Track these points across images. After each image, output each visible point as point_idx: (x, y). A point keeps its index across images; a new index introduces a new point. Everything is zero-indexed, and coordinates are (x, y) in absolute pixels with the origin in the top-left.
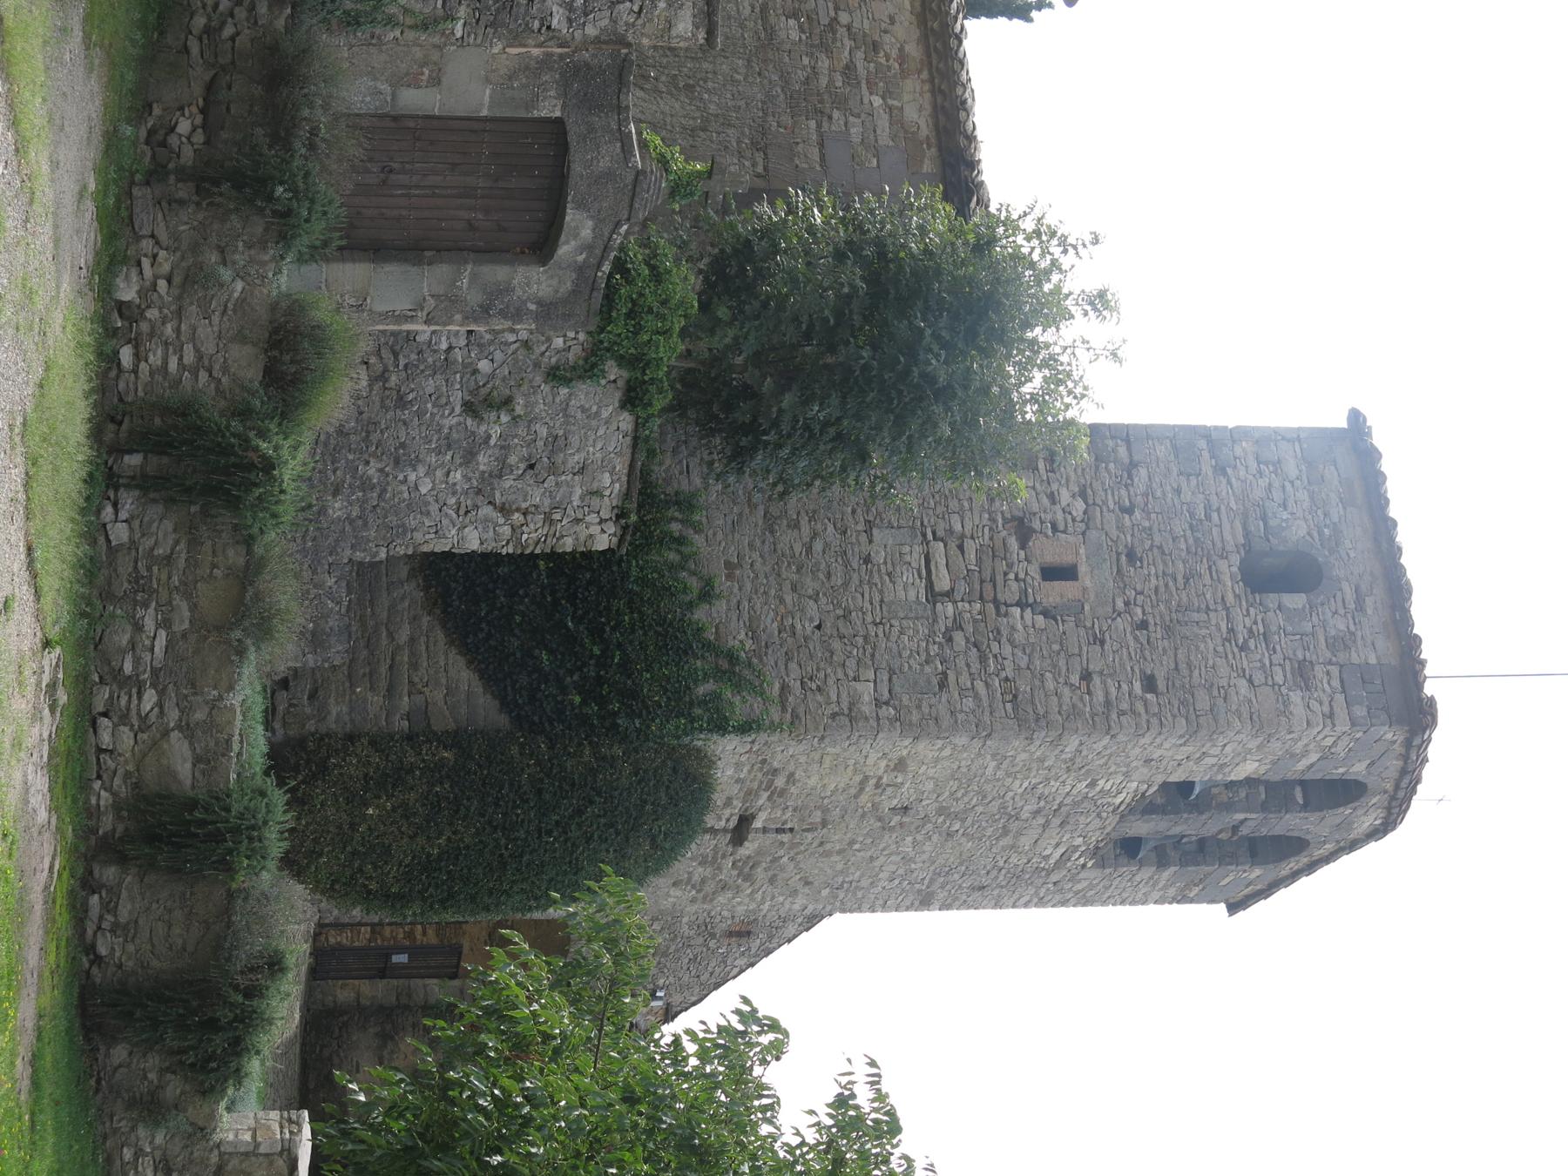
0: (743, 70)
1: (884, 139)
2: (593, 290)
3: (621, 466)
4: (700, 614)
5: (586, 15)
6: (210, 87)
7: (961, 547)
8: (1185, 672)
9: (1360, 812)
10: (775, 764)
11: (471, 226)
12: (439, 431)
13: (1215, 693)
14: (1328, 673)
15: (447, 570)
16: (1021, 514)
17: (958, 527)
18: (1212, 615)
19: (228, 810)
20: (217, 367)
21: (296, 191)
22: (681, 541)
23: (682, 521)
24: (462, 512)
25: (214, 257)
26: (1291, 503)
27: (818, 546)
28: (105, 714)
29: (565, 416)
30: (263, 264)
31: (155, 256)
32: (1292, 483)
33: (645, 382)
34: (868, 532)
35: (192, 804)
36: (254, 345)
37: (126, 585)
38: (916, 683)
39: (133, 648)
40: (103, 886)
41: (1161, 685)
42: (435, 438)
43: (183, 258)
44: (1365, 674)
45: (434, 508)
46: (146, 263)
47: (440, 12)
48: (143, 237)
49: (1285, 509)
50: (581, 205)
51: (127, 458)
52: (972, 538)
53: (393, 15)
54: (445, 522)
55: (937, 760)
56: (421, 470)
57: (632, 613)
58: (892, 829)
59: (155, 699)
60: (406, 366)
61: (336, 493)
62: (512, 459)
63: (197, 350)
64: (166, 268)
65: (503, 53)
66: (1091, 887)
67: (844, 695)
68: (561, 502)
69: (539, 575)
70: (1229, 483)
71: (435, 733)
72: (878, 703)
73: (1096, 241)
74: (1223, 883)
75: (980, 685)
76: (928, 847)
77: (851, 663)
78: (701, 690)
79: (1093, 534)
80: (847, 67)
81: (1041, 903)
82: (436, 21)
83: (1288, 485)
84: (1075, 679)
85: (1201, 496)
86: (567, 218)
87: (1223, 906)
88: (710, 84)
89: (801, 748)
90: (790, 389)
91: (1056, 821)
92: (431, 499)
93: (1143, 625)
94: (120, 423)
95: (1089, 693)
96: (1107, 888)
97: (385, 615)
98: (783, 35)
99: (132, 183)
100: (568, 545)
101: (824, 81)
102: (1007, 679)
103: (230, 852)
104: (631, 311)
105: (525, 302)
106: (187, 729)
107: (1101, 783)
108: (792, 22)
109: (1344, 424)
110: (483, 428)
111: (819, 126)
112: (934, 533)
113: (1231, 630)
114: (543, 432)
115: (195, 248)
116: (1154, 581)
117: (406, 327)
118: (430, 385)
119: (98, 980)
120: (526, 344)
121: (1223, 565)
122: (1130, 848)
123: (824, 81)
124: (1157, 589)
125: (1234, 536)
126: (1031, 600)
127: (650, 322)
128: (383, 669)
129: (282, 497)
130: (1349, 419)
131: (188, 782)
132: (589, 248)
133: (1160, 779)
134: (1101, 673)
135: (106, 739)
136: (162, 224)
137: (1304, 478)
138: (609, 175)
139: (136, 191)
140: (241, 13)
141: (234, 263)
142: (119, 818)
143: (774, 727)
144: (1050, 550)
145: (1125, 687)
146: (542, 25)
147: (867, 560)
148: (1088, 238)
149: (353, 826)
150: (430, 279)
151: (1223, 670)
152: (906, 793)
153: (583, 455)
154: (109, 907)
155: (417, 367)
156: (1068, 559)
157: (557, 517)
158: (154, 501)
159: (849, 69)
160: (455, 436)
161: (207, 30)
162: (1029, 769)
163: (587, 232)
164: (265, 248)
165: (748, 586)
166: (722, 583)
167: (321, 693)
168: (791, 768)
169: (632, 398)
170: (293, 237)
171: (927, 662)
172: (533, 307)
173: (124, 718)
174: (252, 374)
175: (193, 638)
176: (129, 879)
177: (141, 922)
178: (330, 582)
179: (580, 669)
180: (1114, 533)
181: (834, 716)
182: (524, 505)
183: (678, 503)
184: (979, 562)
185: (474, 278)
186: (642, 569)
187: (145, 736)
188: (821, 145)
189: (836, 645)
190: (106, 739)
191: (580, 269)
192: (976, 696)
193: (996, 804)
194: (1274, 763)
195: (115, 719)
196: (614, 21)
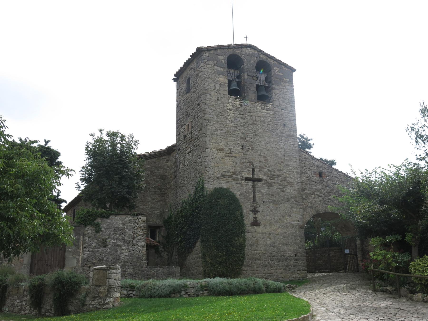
12: (111, 252)
24: (134, 246)
45: (132, 252)
62: (120, 238)
68: (132, 227)
92: (130, 252)
93: (193, 109)
109: (176, 82)
114: (113, 232)
120: (89, 238)
147: (187, 165)
153: (120, 224)
178: (153, 271)
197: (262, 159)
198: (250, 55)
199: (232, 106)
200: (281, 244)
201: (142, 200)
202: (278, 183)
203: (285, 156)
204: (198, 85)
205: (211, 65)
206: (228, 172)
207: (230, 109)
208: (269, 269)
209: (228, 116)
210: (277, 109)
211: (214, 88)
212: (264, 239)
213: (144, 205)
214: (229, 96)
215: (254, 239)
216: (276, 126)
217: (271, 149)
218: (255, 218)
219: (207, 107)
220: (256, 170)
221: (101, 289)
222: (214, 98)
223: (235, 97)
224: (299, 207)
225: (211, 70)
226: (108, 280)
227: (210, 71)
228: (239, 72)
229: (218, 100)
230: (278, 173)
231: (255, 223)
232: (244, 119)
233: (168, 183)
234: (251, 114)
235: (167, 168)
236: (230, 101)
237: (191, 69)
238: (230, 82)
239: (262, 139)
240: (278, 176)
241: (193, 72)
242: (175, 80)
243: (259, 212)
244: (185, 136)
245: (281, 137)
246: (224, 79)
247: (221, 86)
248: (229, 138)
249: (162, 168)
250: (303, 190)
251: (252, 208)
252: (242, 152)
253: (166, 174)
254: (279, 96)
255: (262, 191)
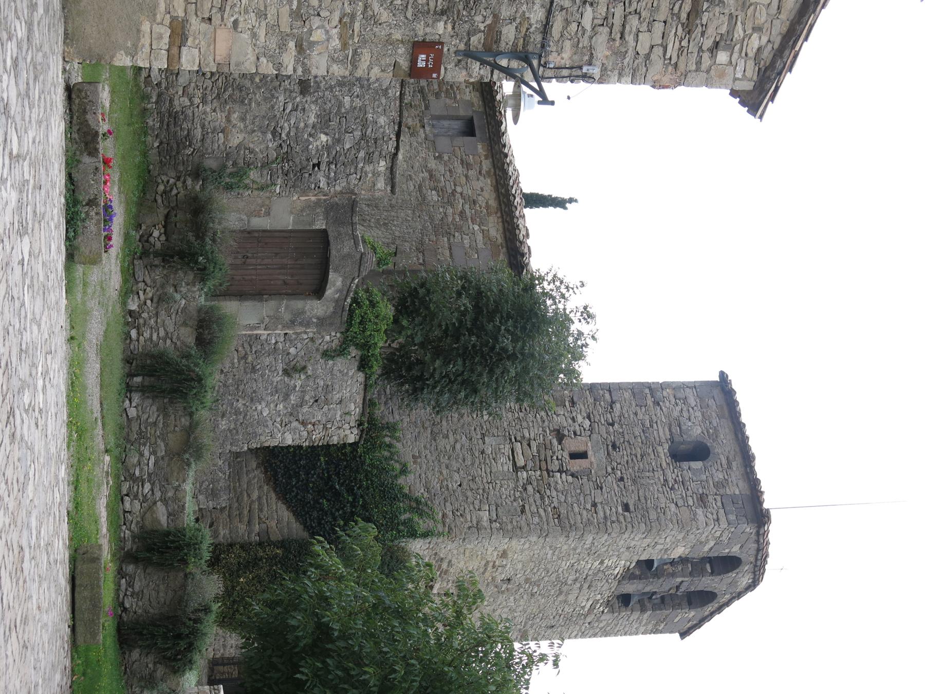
0: (411, 216)
1: (480, 245)
2: (343, 311)
3: (359, 400)
4: (401, 481)
5: (336, 181)
6: (167, 217)
7: (529, 445)
8: (643, 501)
9: (740, 575)
10: (442, 555)
11: (285, 283)
12: (272, 384)
13: (659, 511)
14: (715, 499)
15: (275, 463)
16: (558, 428)
17: (527, 435)
18: (655, 473)
19: (185, 536)
20: (174, 337)
21: (208, 259)
22: (390, 446)
23: (390, 437)
24: (283, 425)
25: (172, 290)
26: (692, 417)
27: (458, 446)
28: (127, 495)
29: (332, 375)
30: (194, 292)
31: (145, 290)
32: (693, 408)
33: (369, 356)
34: (483, 439)
35: (168, 534)
36: (192, 327)
37: (136, 436)
38: (509, 511)
39: (139, 464)
40: (127, 574)
41: (632, 508)
42: (270, 387)
43: (158, 290)
44: (733, 499)
45: (270, 423)
46: (141, 293)
47: (269, 182)
48: (140, 282)
49: (690, 421)
50: (335, 271)
51: (135, 379)
52: (535, 440)
53: (248, 184)
54: (275, 430)
55: (522, 551)
56: (264, 404)
57: (367, 480)
58: (503, 592)
59: (150, 487)
60: (256, 352)
61: (223, 416)
62: (307, 398)
63: (165, 330)
64: (150, 295)
65: (298, 200)
66: (608, 625)
67: (474, 518)
68: (330, 419)
69: (321, 464)
70: (661, 409)
71: (272, 542)
72: (491, 521)
73: (583, 285)
75: (541, 511)
76: (522, 602)
77: (477, 502)
78: (403, 517)
79: (594, 436)
80: (461, 212)
81: (583, 635)
82: (268, 186)
83: (691, 409)
84: (589, 506)
85: (648, 416)
86: (330, 277)
87: (677, 635)
88: (395, 223)
89: (454, 545)
90: (438, 358)
91: (586, 586)
92: (268, 419)
93: (622, 479)
94: (131, 364)
95: (596, 513)
96: (616, 625)
97: (245, 486)
98: (430, 198)
99: (134, 259)
100: (335, 440)
101: (450, 219)
102: (555, 508)
103: (186, 555)
104: (361, 321)
105: (311, 318)
106: (165, 501)
107: (606, 561)
108: (434, 192)
110: (293, 382)
111: (449, 240)
112: (515, 438)
113: (666, 480)
114: (322, 383)
115: (163, 286)
116: (626, 458)
117: (255, 332)
118: (267, 361)
119: (125, 619)
120: (312, 340)
121: (660, 449)
122: (625, 599)
123: (450, 219)
124: (627, 462)
125: (664, 434)
126: (565, 469)
127: (370, 326)
128: (246, 512)
129: (205, 394)
130: (720, 376)
131: (166, 525)
132: (340, 291)
133: (636, 559)
134: (601, 503)
135: (127, 506)
136: (148, 276)
137: (699, 405)
138: (349, 255)
139: (135, 262)
140: (179, 184)
141: (181, 292)
142: (133, 541)
143: (440, 534)
144: (573, 445)
145: (613, 509)
146: (316, 186)
147: (483, 452)
148: (579, 284)
149: (233, 588)
150: (267, 308)
151: (663, 500)
152: (508, 572)
153: (341, 394)
154: (130, 584)
155: (261, 352)
156: (582, 448)
157: (329, 426)
158: (148, 397)
159: (462, 214)
160: (279, 386)
161: (165, 192)
162: (569, 555)
163: (339, 283)
164: (194, 286)
165: (424, 466)
166: (411, 466)
167: (215, 524)
168: (449, 557)
169: (364, 365)
170: (208, 279)
171: (514, 500)
172: (315, 320)
173: (136, 497)
174: (191, 340)
175: (166, 459)
176: (139, 571)
177: (145, 591)
178: (220, 463)
179: (342, 509)
180: (605, 436)
181: (469, 528)
182: (313, 421)
183: (388, 428)
184: (538, 452)
185: (287, 307)
186: (371, 460)
187: (145, 505)
188: (450, 249)
189: (469, 494)
190: (127, 506)
191: (337, 301)
192: (540, 516)
193: (554, 575)
194: (692, 548)
195: (132, 497)
196: (348, 183)
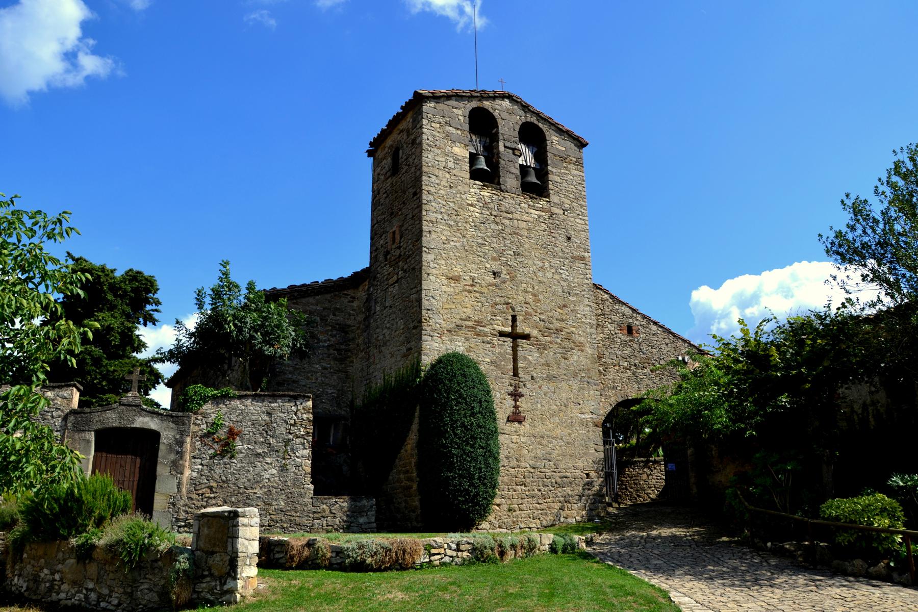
74: (564, 149)
109: (372, 158)
147: (391, 307)
185: (164, 458)
197: (530, 298)
198: (510, 113)
199: (476, 199)
200: (562, 455)
201: (304, 369)
202: (557, 343)
203: (569, 294)
204: (414, 159)
205: (440, 123)
206: (468, 319)
207: (472, 205)
208: (540, 502)
209: (469, 216)
210: (555, 210)
211: (443, 166)
212: (531, 447)
213: (308, 378)
214: (472, 181)
215: (514, 446)
216: (554, 239)
217: (545, 280)
218: (516, 407)
219: (431, 198)
220: (520, 318)
221: (216, 559)
222: (444, 183)
223: (482, 184)
224: (595, 387)
225: (439, 132)
226: (230, 540)
227: (437, 134)
228: (488, 141)
229: (451, 187)
230: (557, 325)
231: (516, 418)
232: (497, 223)
233: (353, 339)
234: (510, 216)
235: (351, 312)
236: (472, 190)
237: (402, 131)
238: (473, 158)
239: (530, 262)
240: (558, 331)
241: (405, 137)
242: (370, 153)
243: (523, 396)
244: (387, 253)
245: (562, 260)
246: (462, 149)
247: (457, 162)
248: (470, 257)
249: (342, 312)
250: (600, 358)
251: (511, 389)
252: (496, 285)
253: (348, 322)
254: (559, 187)
255: (530, 358)
